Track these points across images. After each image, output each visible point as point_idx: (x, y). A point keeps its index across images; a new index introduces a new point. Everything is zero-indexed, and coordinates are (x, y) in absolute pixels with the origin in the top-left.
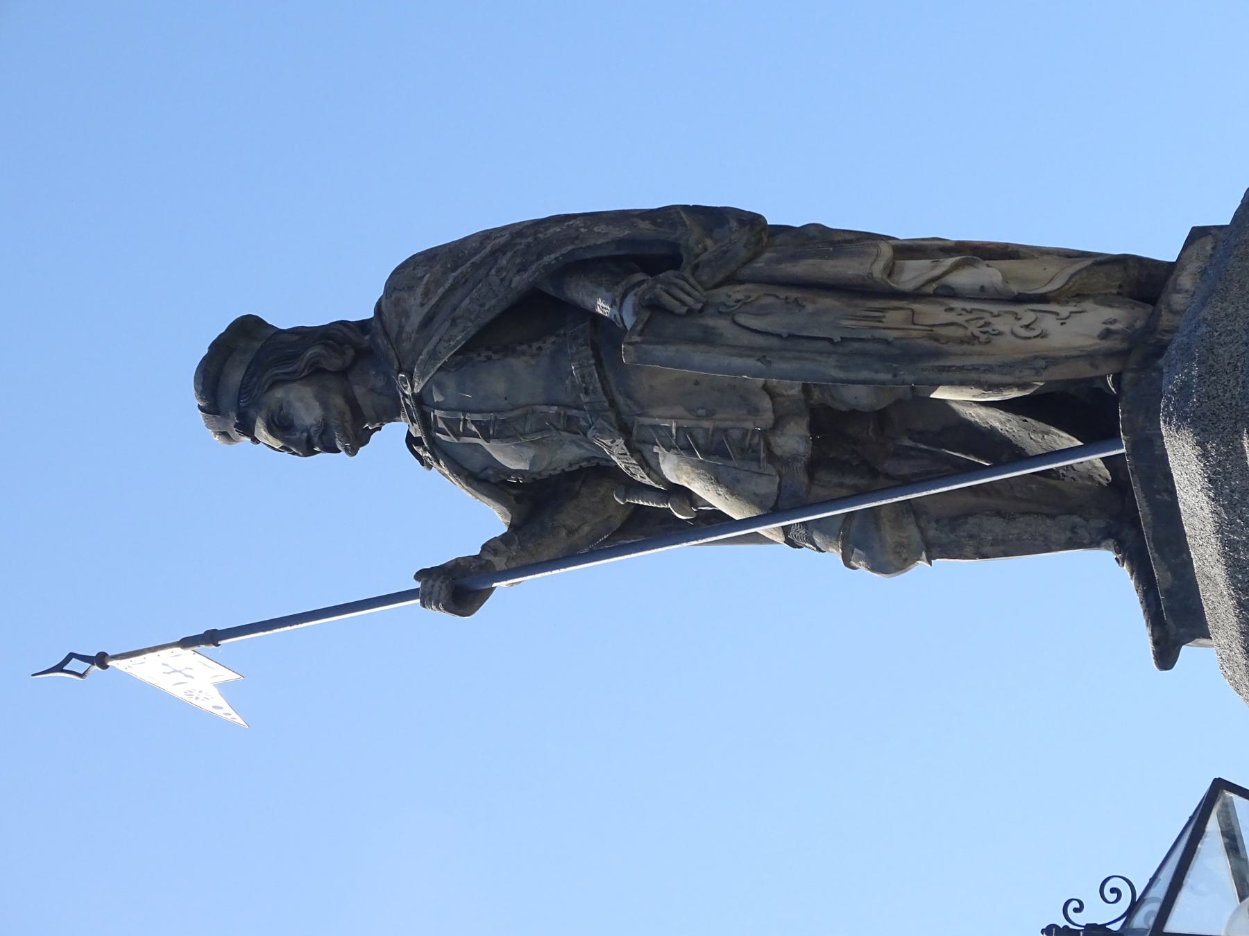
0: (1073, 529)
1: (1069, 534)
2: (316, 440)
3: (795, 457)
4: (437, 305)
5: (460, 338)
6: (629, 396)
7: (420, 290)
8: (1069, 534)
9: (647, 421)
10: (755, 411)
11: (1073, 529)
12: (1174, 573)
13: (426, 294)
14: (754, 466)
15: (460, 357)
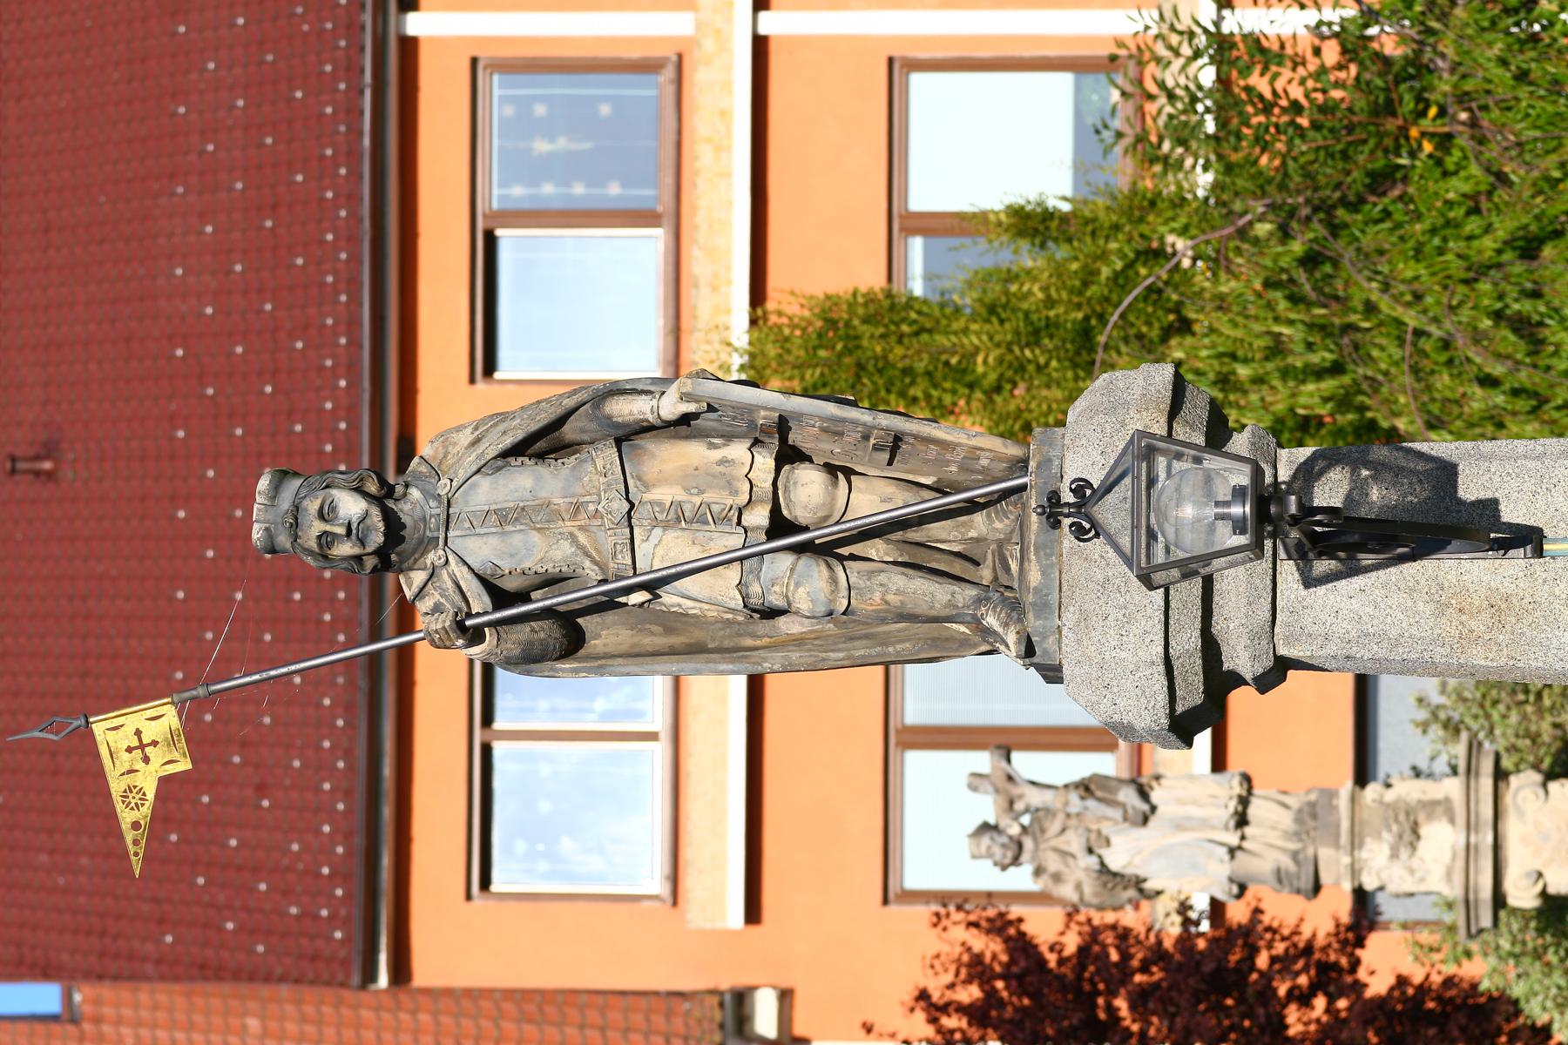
0: (953, 594)
1: (949, 597)
2: (354, 526)
3: (758, 528)
4: (487, 430)
5: (508, 441)
6: (639, 478)
7: (469, 430)
8: (949, 597)
9: (648, 497)
10: (735, 493)
11: (953, 594)
12: (1043, 573)
13: (476, 429)
14: (728, 529)
15: (500, 463)
